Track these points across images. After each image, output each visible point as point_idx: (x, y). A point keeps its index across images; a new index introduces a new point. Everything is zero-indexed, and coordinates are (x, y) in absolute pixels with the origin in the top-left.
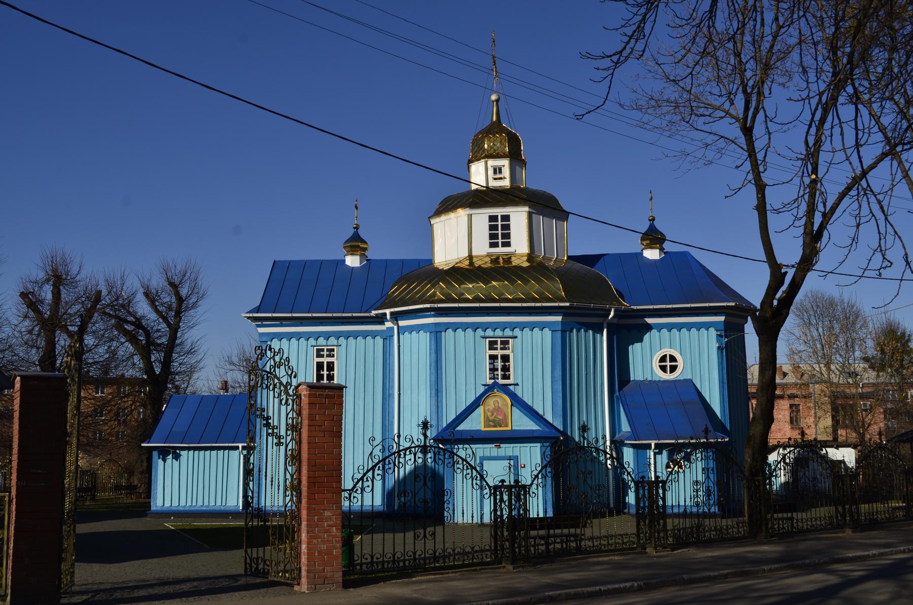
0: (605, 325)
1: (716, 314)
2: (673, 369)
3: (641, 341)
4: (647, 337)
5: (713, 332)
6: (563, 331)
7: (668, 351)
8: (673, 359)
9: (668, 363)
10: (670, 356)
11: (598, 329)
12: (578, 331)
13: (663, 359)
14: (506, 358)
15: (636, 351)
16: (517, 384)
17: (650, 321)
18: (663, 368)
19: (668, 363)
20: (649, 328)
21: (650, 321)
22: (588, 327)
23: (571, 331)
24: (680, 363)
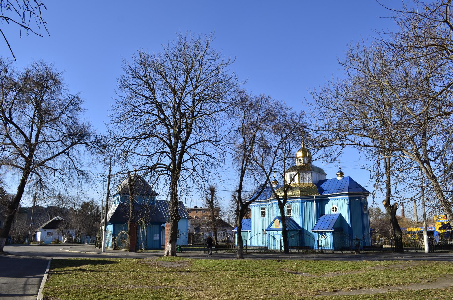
2: (336, 210)
4: (329, 202)
5: (346, 200)
6: (302, 203)
7: (334, 206)
8: (336, 208)
9: (334, 209)
11: (312, 201)
13: (333, 208)
15: (326, 206)
17: (329, 198)
18: (333, 211)
19: (334, 209)
20: (329, 200)
21: (329, 198)
22: (309, 201)
24: (337, 209)
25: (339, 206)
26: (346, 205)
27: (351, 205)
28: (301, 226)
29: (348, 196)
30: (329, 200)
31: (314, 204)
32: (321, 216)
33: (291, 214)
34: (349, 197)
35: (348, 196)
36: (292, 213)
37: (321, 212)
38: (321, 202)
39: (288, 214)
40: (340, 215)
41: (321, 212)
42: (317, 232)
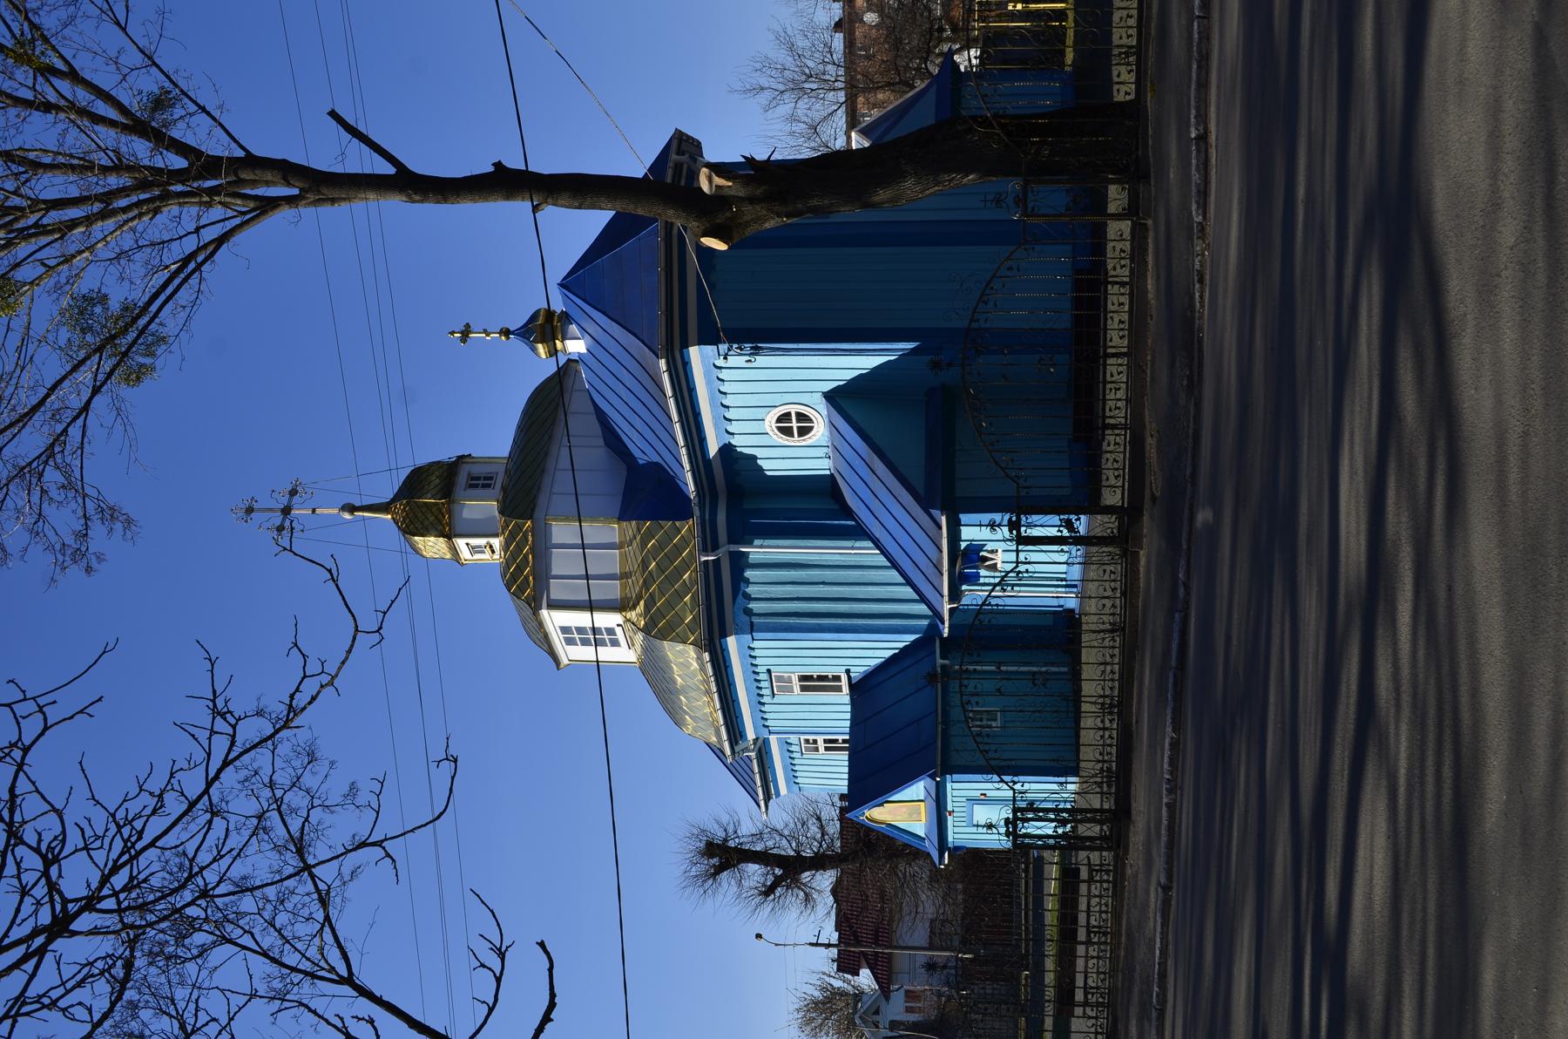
0: (733, 548)
1: (686, 364)
2: (801, 417)
3: (754, 458)
6: (752, 629)
9: (794, 425)
10: (779, 420)
11: (740, 563)
12: (748, 598)
13: (787, 432)
14: (803, 678)
16: (848, 672)
17: (713, 449)
20: (727, 450)
21: (713, 449)
22: (739, 580)
23: (749, 612)
25: (772, 403)
26: (761, 360)
27: (755, 334)
28: (912, 637)
29: (694, 352)
30: (727, 450)
31: (757, 551)
32: (848, 513)
33: (837, 678)
34: (703, 341)
35: (694, 352)
36: (830, 672)
37: (815, 507)
38: (745, 500)
39: (839, 689)
40: (830, 397)
41: (815, 507)
42: (955, 595)
